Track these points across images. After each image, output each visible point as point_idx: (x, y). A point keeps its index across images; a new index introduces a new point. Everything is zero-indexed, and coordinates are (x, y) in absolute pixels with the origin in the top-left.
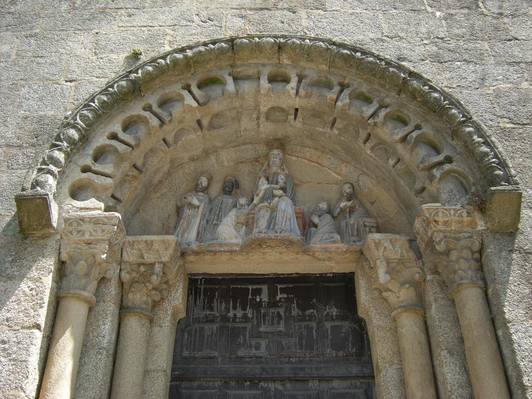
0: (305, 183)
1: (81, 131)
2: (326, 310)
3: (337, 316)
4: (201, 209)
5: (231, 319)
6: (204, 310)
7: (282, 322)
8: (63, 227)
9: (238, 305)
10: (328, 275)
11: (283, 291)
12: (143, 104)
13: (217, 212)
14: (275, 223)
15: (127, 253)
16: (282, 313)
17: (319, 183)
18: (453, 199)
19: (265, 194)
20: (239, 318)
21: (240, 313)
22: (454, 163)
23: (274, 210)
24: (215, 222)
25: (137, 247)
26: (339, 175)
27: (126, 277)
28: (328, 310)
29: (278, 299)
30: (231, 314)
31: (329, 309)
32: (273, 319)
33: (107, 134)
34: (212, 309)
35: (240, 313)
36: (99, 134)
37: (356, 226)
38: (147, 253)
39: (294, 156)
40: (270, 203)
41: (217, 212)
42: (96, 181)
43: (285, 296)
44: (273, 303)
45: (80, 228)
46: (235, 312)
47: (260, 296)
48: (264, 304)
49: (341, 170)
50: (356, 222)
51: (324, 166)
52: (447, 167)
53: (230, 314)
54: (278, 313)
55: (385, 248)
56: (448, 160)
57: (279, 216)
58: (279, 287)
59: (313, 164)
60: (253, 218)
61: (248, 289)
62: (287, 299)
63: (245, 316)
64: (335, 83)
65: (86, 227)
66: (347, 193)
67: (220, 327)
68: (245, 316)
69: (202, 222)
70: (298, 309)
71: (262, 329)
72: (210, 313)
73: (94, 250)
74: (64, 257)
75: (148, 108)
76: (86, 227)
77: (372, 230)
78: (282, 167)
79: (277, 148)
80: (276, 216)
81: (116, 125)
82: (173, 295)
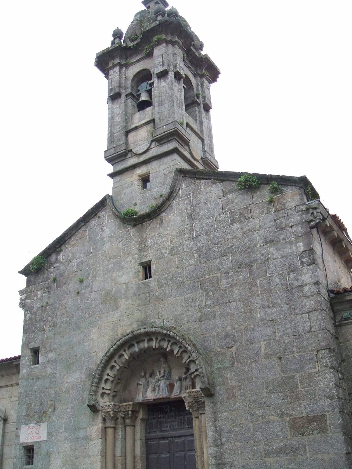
7: (173, 418)
35: (162, 416)
44: (171, 411)
52: (196, 373)
57: (161, 388)
68: (163, 417)
71: (168, 420)
75: (115, 362)
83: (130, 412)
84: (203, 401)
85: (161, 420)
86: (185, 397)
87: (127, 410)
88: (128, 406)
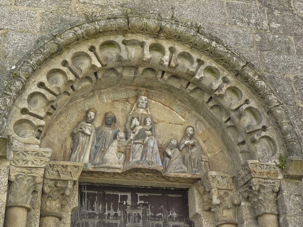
0: (161, 122)
1: (23, 83)
2: (169, 214)
3: (176, 218)
4: (91, 138)
5: (106, 217)
6: (88, 209)
7: (141, 221)
8: (12, 156)
9: (111, 207)
10: (171, 189)
11: (141, 198)
12: (61, 60)
13: (104, 142)
14: (146, 155)
15: (49, 173)
16: (141, 215)
17: (170, 123)
18: (265, 156)
19: (139, 133)
20: (112, 216)
21: (112, 213)
22: (267, 132)
23: (145, 145)
24: (103, 150)
25: (56, 169)
26: (183, 118)
27: (47, 190)
28: (170, 214)
29: (138, 203)
30: (106, 213)
31: (172, 213)
32: (135, 218)
33: (37, 83)
34: (93, 209)
35: (112, 213)
36: (31, 83)
37: (196, 160)
38: (63, 174)
39: (154, 100)
40: (143, 141)
41: (104, 142)
42: (33, 122)
43: (143, 202)
44: (135, 206)
45: (25, 158)
46: (109, 212)
47: (126, 201)
48: (128, 206)
49: (185, 114)
50: (196, 158)
51: (173, 110)
52: (263, 134)
53: (105, 213)
54: (138, 214)
55: (218, 181)
56: (264, 128)
57: (149, 151)
58: (139, 195)
59: (166, 107)
60: (130, 149)
61: (118, 195)
62: (144, 205)
63: (116, 215)
64: (195, 60)
65: (29, 157)
66: (190, 134)
67: (99, 222)
68: (116, 215)
69: (92, 147)
70: (152, 212)
72: (92, 212)
73: (34, 175)
74: (13, 178)
75: (65, 63)
76: (29, 157)
77: (206, 164)
78: (146, 109)
79: (145, 95)
80: (147, 151)
81: (43, 76)
82: (72, 200)
83: (70, 185)
84: (277, 189)
85: (114, 222)
86: (214, 178)
87: (63, 177)
88: (69, 169)
